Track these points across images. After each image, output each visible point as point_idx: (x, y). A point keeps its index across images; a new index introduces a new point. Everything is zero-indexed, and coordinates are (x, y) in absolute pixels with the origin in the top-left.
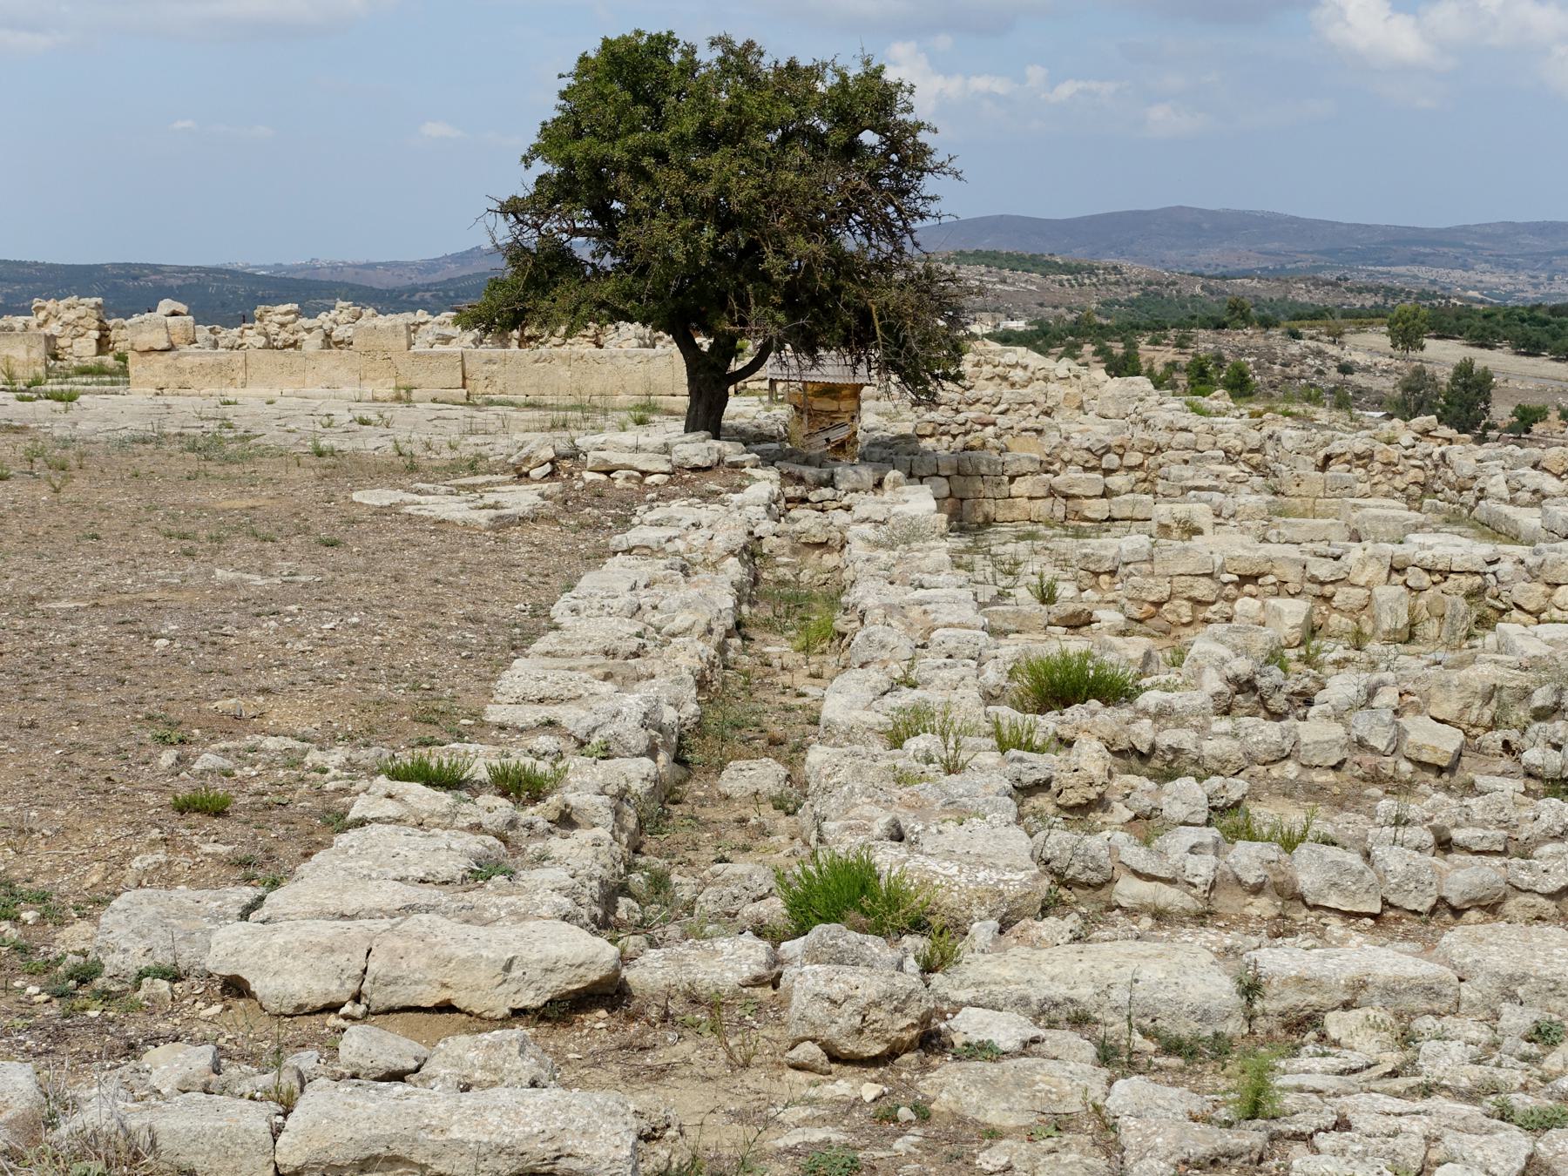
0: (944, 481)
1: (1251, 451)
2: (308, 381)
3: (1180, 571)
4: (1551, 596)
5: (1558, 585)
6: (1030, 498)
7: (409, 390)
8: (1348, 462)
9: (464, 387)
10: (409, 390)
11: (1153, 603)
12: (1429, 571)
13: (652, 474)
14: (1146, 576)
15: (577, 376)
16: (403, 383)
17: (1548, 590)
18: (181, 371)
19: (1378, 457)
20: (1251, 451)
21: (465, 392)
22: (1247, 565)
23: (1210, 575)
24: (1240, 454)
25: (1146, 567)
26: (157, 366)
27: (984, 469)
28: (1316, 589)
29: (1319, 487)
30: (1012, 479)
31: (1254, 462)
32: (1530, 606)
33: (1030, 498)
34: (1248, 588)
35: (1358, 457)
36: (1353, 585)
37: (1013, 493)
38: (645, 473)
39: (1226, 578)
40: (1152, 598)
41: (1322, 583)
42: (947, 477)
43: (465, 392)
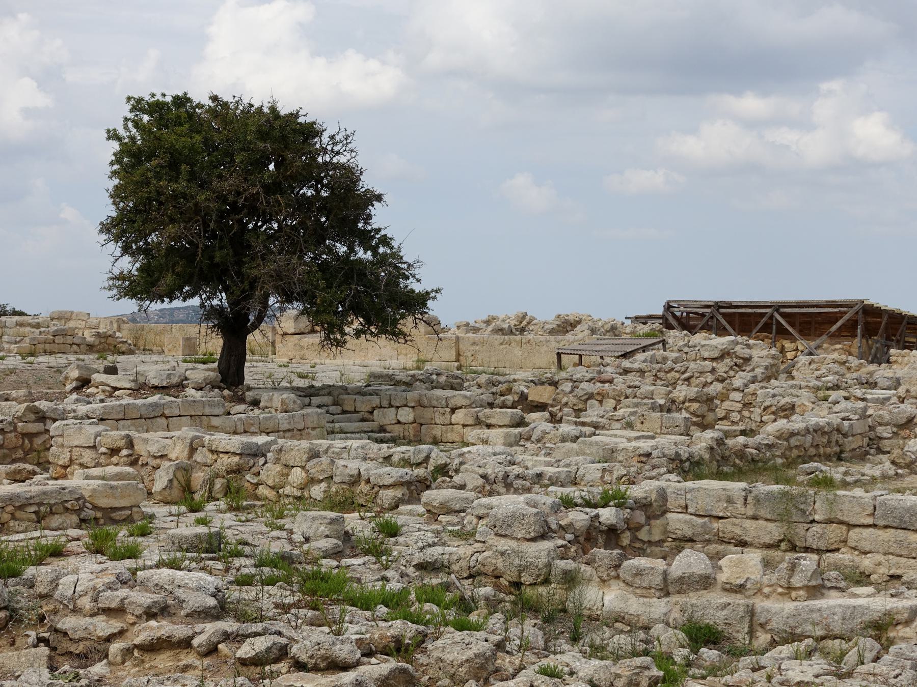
0: (411, 410)
1: (690, 401)
2: (369, 356)
3: (76, 443)
4: (288, 475)
5: (293, 467)
6: (464, 426)
7: (424, 361)
8: (773, 413)
9: (457, 360)
10: (424, 361)
11: (61, 466)
12: (212, 452)
13: (120, 389)
14: (58, 447)
15: (526, 354)
16: (422, 357)
17: (286, 470)
18: (302, 347)
19: (798, 410)
20: (690, 401)
21: (456, 364)
22: (109, 440)
23: (94, 447)
24: (684, 403)
25: (60, 440)
26: (290, 344)
27: (435, 403)
28: (150, 461)
29: (657, 425)
30: (453, 411)
31: (692, 409)
32: (270, 483)
33: (464, 426)
34: (115, 459)
35: (783, 409)
36: (170, 460)
37: (453, 421)
38: (116, 389)
39: (103, 450)
40: (60, 463)
41: (156, 457)
42: (413, 407)
43: (456, 364)
